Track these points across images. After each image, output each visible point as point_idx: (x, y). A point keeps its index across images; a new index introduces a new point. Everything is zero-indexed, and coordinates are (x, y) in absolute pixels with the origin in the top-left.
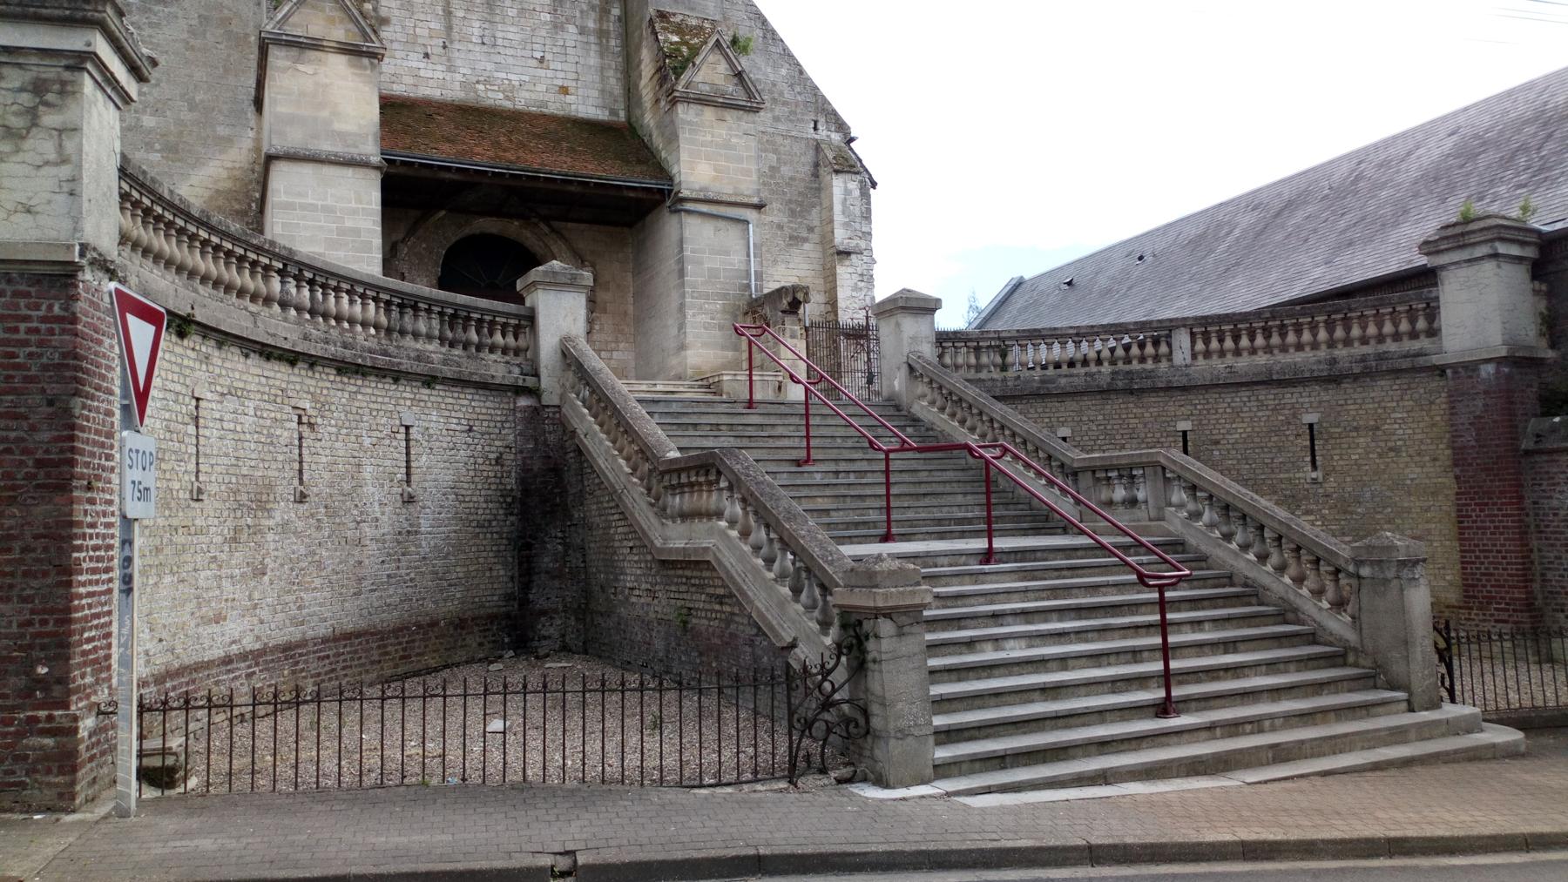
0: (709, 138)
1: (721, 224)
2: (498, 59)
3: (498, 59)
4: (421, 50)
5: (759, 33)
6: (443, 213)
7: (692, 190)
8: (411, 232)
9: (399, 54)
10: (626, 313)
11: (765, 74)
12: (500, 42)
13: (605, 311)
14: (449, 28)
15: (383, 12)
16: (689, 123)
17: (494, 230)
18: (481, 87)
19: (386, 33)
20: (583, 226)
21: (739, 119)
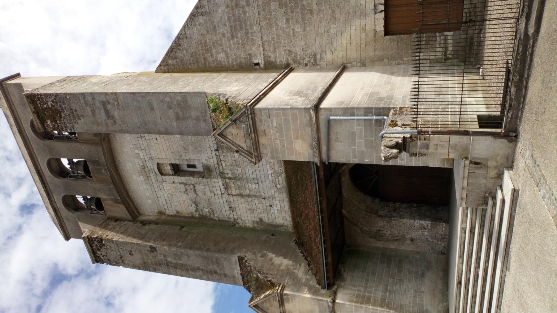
0: (278, 141)
1: (333, 137)
2: (263, 177)
3: (263, 177)
4: (269, 208)
5: (201, 19)
6: (344, 212)
7: (314, 156)
9: (274, 216)
11: (223, 12)
12: (255, 176)
14: (256, 196)
15: (258, 220)
16: (272, 153)
18: (278, 186)
19: (266, 219)
21: (261, 121)
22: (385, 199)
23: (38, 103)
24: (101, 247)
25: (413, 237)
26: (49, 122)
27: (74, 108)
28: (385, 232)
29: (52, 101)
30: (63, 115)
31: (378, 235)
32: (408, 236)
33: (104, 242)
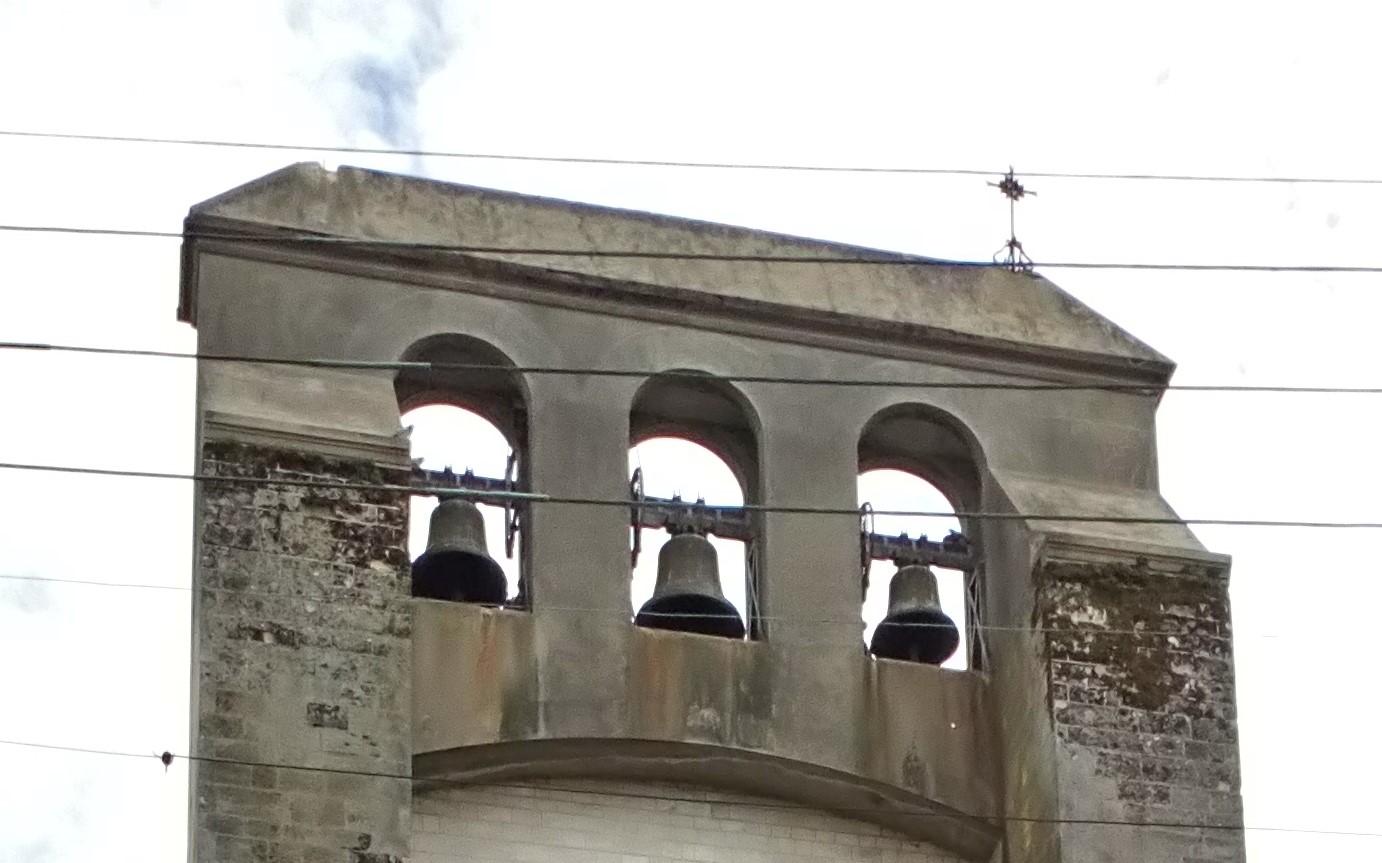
23: (1187, 613)
24: (337, 528)
26: (1096, 616)
27: (1173, 789)
29: (1199, 695)
30: (1138, 714)
33: (378, 566)
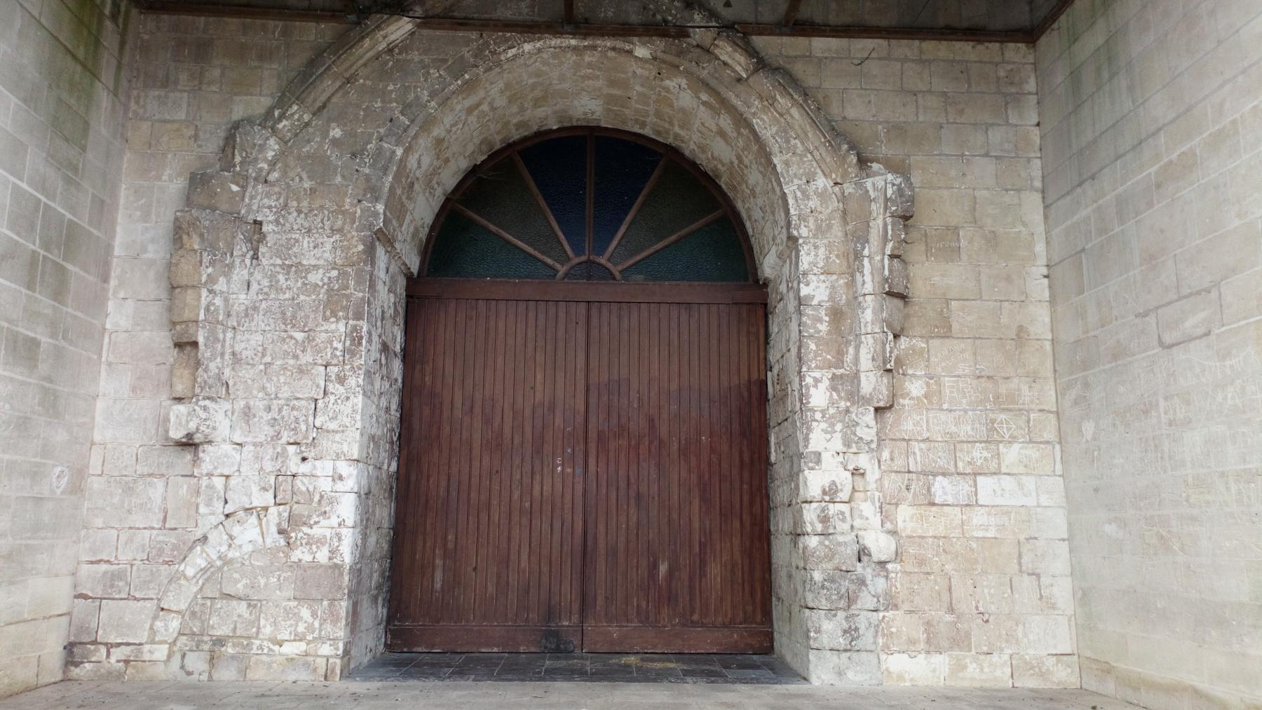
6: (400, 28)
8: (297, 87)
10: (1021, 336)
13: (944, 330)
17: (588, 106)
20: (862, 46)
22: (419, 300)
25: (208, 455)
28: (239, 274)
31: (209, 219)
32: (219, 420)
